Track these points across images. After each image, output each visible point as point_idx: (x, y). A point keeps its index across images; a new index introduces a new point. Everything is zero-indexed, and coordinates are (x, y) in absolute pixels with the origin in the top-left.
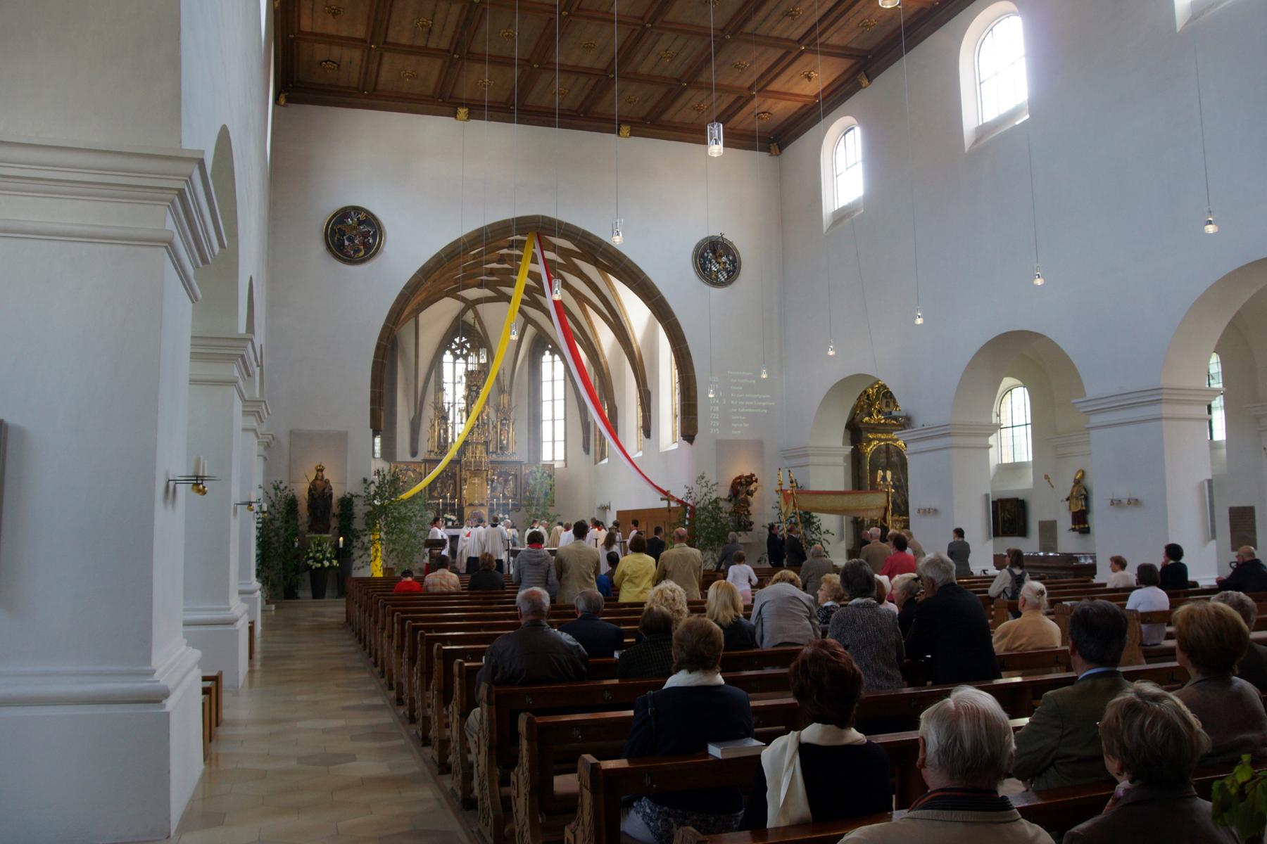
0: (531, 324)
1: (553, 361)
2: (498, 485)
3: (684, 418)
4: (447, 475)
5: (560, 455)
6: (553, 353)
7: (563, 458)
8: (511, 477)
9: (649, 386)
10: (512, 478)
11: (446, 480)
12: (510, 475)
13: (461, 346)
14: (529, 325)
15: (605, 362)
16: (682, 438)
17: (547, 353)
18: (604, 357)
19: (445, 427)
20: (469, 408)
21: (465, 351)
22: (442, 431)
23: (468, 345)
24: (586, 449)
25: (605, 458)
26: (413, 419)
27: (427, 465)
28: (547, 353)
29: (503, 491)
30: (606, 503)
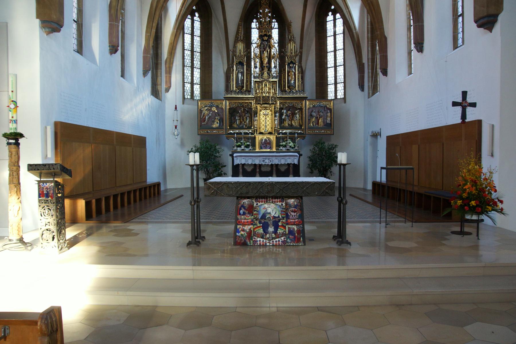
1: (335, 20)
2: (287, 117)
4: (244, 109)
5: (340, 95)
7: (343, 97)
10: (299, 112)
11: (243, 114)
12: (297, 109)
13: (265, 15)
17: (330, 13)
19: (242, 71)
21: (268, 19)
23: (270, 15)
24: (362, 87)
25: (377, 92)
26: (226, 72)
28: (330, 13)
29: (291, 122)
30: (376, 130)
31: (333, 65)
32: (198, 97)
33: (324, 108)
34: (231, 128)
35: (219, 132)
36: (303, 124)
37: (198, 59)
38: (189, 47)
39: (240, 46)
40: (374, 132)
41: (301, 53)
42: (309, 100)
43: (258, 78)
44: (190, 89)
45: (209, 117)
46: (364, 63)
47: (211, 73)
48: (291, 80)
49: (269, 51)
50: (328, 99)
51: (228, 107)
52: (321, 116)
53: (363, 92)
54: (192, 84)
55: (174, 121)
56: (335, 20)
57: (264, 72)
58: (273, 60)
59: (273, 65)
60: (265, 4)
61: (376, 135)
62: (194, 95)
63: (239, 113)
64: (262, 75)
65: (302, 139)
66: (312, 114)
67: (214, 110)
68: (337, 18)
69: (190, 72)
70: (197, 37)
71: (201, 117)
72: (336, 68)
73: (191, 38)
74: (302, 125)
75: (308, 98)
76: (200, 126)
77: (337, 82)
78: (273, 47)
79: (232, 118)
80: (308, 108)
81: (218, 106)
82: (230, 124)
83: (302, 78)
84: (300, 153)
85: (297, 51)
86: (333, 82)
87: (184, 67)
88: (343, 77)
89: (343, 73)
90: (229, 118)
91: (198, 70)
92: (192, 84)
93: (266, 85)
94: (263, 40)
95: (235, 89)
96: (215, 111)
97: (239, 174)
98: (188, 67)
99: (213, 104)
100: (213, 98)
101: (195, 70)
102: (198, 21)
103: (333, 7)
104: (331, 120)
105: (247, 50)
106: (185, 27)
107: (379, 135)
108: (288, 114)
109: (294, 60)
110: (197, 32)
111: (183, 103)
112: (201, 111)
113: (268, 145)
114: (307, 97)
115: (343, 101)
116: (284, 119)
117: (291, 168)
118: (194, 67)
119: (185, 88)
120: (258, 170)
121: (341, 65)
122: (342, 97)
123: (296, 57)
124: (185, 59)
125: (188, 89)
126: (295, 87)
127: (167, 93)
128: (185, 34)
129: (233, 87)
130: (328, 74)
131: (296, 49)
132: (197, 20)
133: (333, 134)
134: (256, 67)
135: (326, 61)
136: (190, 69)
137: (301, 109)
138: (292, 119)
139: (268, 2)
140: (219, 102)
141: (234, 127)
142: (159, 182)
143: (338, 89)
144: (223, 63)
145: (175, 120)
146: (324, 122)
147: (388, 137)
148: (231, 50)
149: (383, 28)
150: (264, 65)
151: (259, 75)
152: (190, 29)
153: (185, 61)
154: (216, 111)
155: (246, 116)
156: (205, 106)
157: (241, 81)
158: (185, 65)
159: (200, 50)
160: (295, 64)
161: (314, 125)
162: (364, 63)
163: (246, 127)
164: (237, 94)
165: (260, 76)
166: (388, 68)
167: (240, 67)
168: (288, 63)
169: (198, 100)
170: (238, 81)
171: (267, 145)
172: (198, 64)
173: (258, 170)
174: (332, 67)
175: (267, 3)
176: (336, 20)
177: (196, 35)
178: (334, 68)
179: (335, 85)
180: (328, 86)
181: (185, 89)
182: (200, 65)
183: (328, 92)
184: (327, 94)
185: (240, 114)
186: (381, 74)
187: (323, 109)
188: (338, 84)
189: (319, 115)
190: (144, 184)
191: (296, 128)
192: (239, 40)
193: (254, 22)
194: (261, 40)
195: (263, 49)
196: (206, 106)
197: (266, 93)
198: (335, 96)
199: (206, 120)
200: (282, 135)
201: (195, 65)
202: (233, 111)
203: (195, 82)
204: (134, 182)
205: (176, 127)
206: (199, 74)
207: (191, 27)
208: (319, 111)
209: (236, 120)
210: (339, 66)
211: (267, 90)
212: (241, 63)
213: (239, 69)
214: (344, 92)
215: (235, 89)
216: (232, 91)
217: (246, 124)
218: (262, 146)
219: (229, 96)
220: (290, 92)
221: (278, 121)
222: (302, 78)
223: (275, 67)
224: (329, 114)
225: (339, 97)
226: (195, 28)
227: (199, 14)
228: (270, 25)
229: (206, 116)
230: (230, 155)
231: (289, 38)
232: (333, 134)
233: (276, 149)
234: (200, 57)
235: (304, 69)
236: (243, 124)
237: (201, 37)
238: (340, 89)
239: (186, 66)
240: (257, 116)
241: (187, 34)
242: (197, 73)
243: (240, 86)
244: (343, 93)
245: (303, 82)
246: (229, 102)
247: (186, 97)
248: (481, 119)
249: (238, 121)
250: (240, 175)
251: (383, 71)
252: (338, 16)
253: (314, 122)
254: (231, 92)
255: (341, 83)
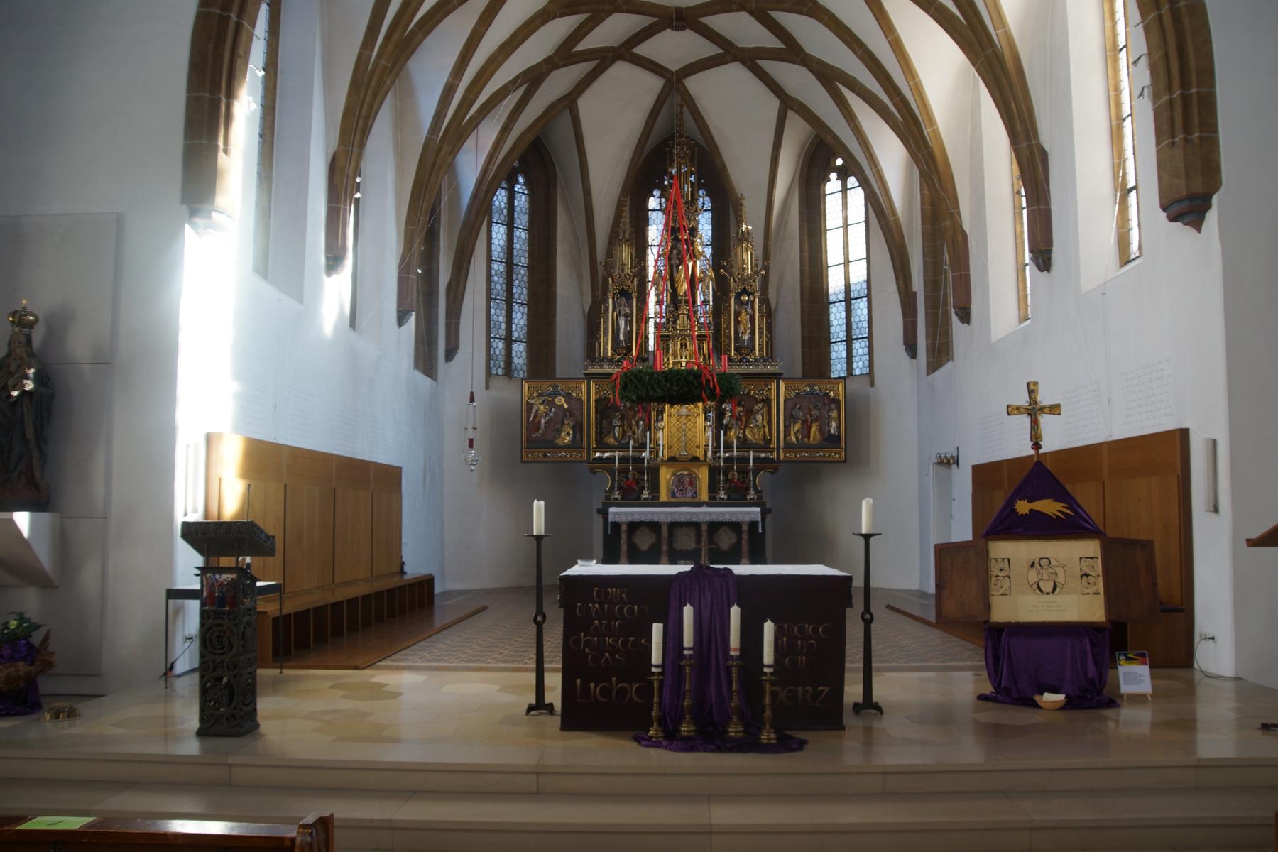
0: (792, 109)
1: (845, 190)
2: (733, 421)
3: (1173, 144)
5: (860, 366)
6: (843, 174)
7: (866, 371)
8: (760, 405)
9: (1046, 137)
14: (789, 111)
15: (936, 133)
16: (1164, 215)
17: (833, 176)
18: (932, 122)
20: (675, 275)
22: (622, 322)
23: (692, 179)
24: (911, 349)
26: (588, 313)
27: (592, 385)
28: (833, 176)
29: (744, 432)
30: (948, 450)
31: (841, 297)
32: (521, 372)
33: (824, 400)
34: (602, 446)
35: (571, 456)
36: (773, 439)
37: (522, 283)
38: (502, 254)
39: (625, 254)
40: (943, 456)
41: (766, 268)
42: (785, 380)
43: (665, 328)
44: (503, 352)
45: (549, 420)
46: (915, 293)
47: (554, 316)
48: (742, 333)
49: (690, 264)
50: (832, 377)
51: (593, 398)
52: (815, 417)
53: (914, 360)
54: (509, 341)
55: (466, 429)
56: (845, 190)
57: (679, 314)
58: (701, 284)
59: (700, 298)
60: (682, 155)
61: (948, 462)
62: (513, 368)
63: (619, 410)
64: (675, 322)
65: (772, 473)
66: (794, 413)
67: (560, 403)
68: (849, 187)
69: (504, 312)
70: (521, 231)
71: (531, 419)
72: (851, 304)
73: (506, 232)
74: (771, 439)
75: (783, 376)
76: (528, 441)
77: (852, 336)
78: (701, 255)
79: (604, 422)
80: (785, 401)
81: (570, 394)
82: (598, 435)
83: (770, 328)
84: (768, 506)
85: (756, 265)
86: (842, 335)
87: (491, 302)
88: (865, 324)
89: (867, 316)
90: (596, 424)
91: (521, 308)
92: (509, 341)
93: (683, 346)
94: (676, 240)
95: (610, 355)
96: (563, 404)
97: (620, 557)
98: (498, 301)
99: (559, 389)
100: (558, 376)
101: (516, 307)
102: (523, 194)
103: (839, 162)
104: (839, 427)
105: (639, 263)
106: (493, 207)
107: (954, 463)
108: (737, 413)
109: (751, 286)
110: (522, 220)
111: (487, 387)
112: (530, 406)
113: (689, 488)
114: (782, 373)
115: (867, 380)
116: (727, 425)
117: (744, 542)
118: (514, 300)
119: (492, 350)
120: (665, 547)
121: (862, 295)
122: (865, 373)
123: (754, 281)
124: (493, 283)
125: (497, 352)
126: (754, 349)
127: (449, 363)
128: (493, 224)
129: (606, 350)
130: (832, 317)
131: (755, 260)
132: (520, 191)
133: (845, 461)
134: (659, 303)
135: (825, 286)
136: (505, 308)
137: (767, 401)
138: (746, 426)
139: (688, 152)
140: (571, 384)
141: (607, 444)
142: (431, 575)
143: (854, 352)
144: (582, 293)
145: (470, 426)
146: (821, 431)
147: (979, 471)
148: (601, 263)
149: (959, 214)
150: (680, 298)
151: (668, 322)
152: (505, 211)
153: (492, 287)
154: (566, 406)
155: (636, 419)
156: (540, 394)
157: (624, 335)
158: (493, 297)
159: (528, 261)
160: (752, 294)
161: (800, 437)
162: (915, 293)
163: (637, 445)
164: (616, 366)
165: (671, 323)
166: (972, 306)
167: (623, 303)
168: (736, 293)
169: (522, 379)
170: (618, 335)
171: (686, 489)
172: (522, 293)
173: (665, 547)
174: (840, 301)
175: (686, 155)
176: (848, 191)
177: (520, 227)
178: (843, 303)
179: (847, 344)
180: (830, 346)
181: (492, 353)
182: (526, 297)
183: (831, 359)
184: (830, 366)
185: (622, 413)
186: (955, 319)
187: (820, 402)
188: (854, 341)
189: (811, 416)
190: (394, 582)
191: (757, 448)
192: (621, 240)
193: (654, 196)
194: (672, 239)
195: (677, 261)
196: (540, 395)
197: (684, 364)
198: (847, 370)
199: (540, 426)
200: (724, 463)
201: (516, 296)
202: (604, 408)
203: (515, 334)
204: (374, 575)
205: (471, 446)
206: (525, 317)
207: (507, 207)
208: (811, 407)
209: (612, 428)
210: (856, 298)
211: (688, 357)
212: (625, 294)
213: (622, 308)
214: (869, 361)
215: (610, 355)
216: (604, 358)
217: (636, 436)
218: (675, 491)
219: (597, 370)
220: (741, 361)
221: (712, 431)
222: (770, 328)
223: (705, 302)
224: (834, 414)
225: (857, 372)
226: (518, 209)
227: (524, 177)
228: (694, 204)
229: (541, 416)
230: (599, 511)
231: (737, 238)
232: (845, 461)
233: (710, 498)
234: (529, 277)
235: (773, 307)
236: (630, 436)
237: (530, 230)
238: (860, 352)
239: (496, 299)
240: (662, 419)
241: (497, 223)
242: (519, 315)
243: (622, 347)
244: (867, 363)
245: (771, 336)
246: (596, 385)
247: (494, 372)
248: (1187, 427)
249: (617, 428)
250: (622, 558)
251: (960, 313)
252: (852, 181)
253: (798, 431)
254: (602, 360)
255: (863, 338)
